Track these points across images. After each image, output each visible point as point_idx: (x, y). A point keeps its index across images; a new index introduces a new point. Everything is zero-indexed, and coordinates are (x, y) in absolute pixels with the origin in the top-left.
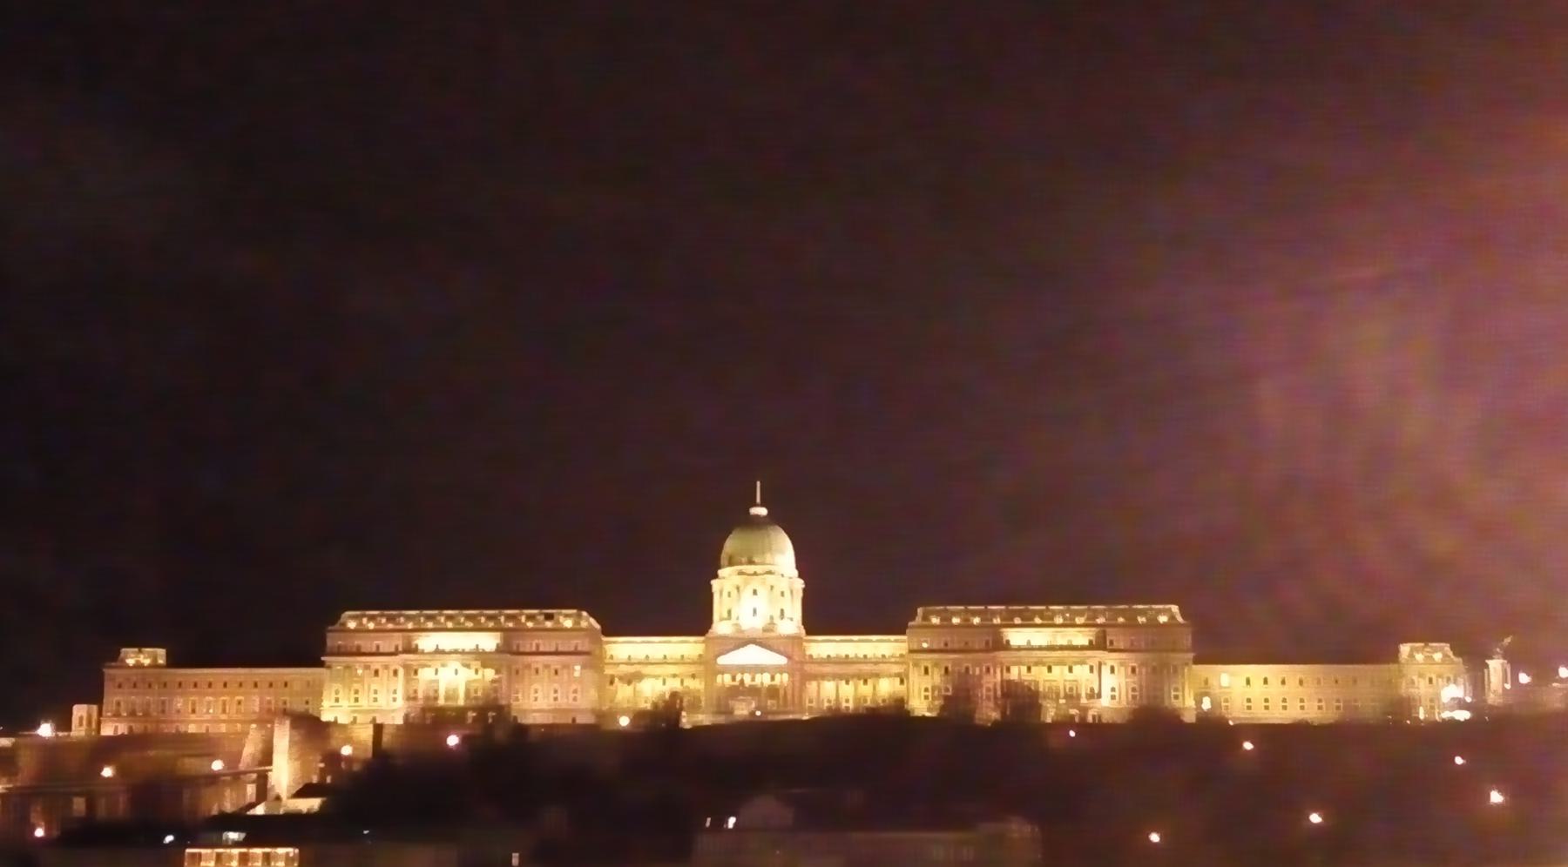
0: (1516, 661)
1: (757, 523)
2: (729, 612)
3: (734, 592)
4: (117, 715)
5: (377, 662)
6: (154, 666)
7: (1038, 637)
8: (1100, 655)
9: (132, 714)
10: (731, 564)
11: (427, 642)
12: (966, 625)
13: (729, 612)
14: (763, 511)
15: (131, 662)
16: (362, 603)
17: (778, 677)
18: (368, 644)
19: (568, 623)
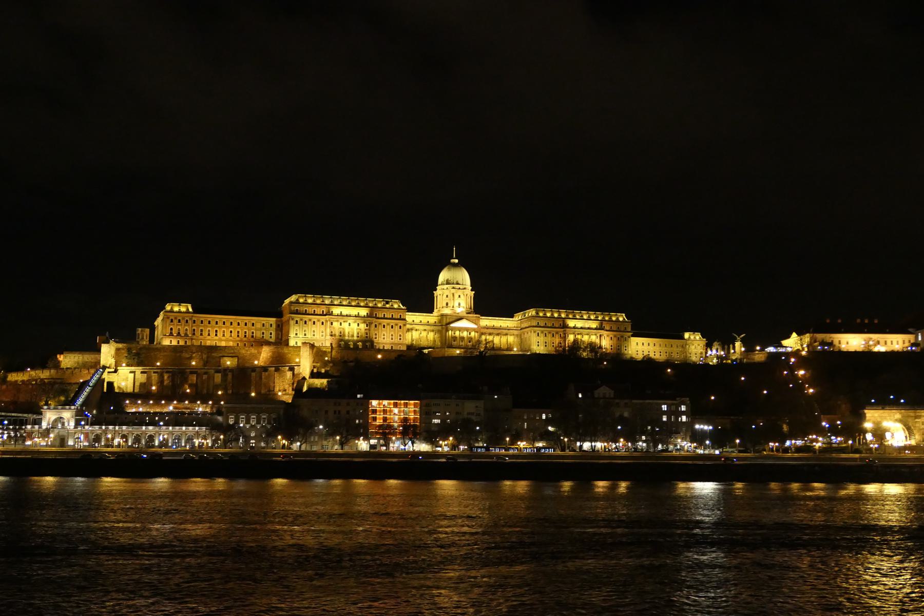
0: (744, 342)
1: (455, 265)
2: (447, 304)
3: (450, 296)
4: (171, 334)
5: (314, 318)
6: (188, 312)
7: (579, 324)
8: (602, 332)
9: (179, 334)
10: (448, 283)
11: (336, 311)
12: (552, 317)
13: (447, 304)
14: (456, 261)
15: (176, 309)
16: (305, 291)
17: (473, 334)
18: (310, 310)
19: (396, 306)
